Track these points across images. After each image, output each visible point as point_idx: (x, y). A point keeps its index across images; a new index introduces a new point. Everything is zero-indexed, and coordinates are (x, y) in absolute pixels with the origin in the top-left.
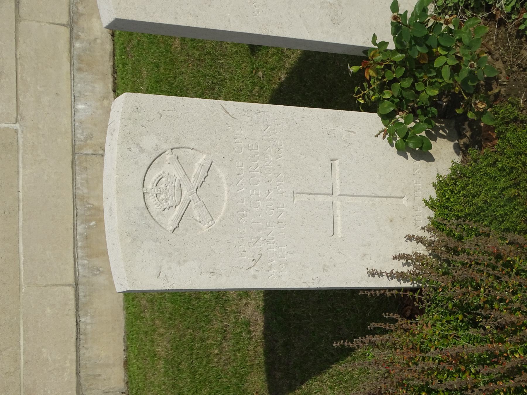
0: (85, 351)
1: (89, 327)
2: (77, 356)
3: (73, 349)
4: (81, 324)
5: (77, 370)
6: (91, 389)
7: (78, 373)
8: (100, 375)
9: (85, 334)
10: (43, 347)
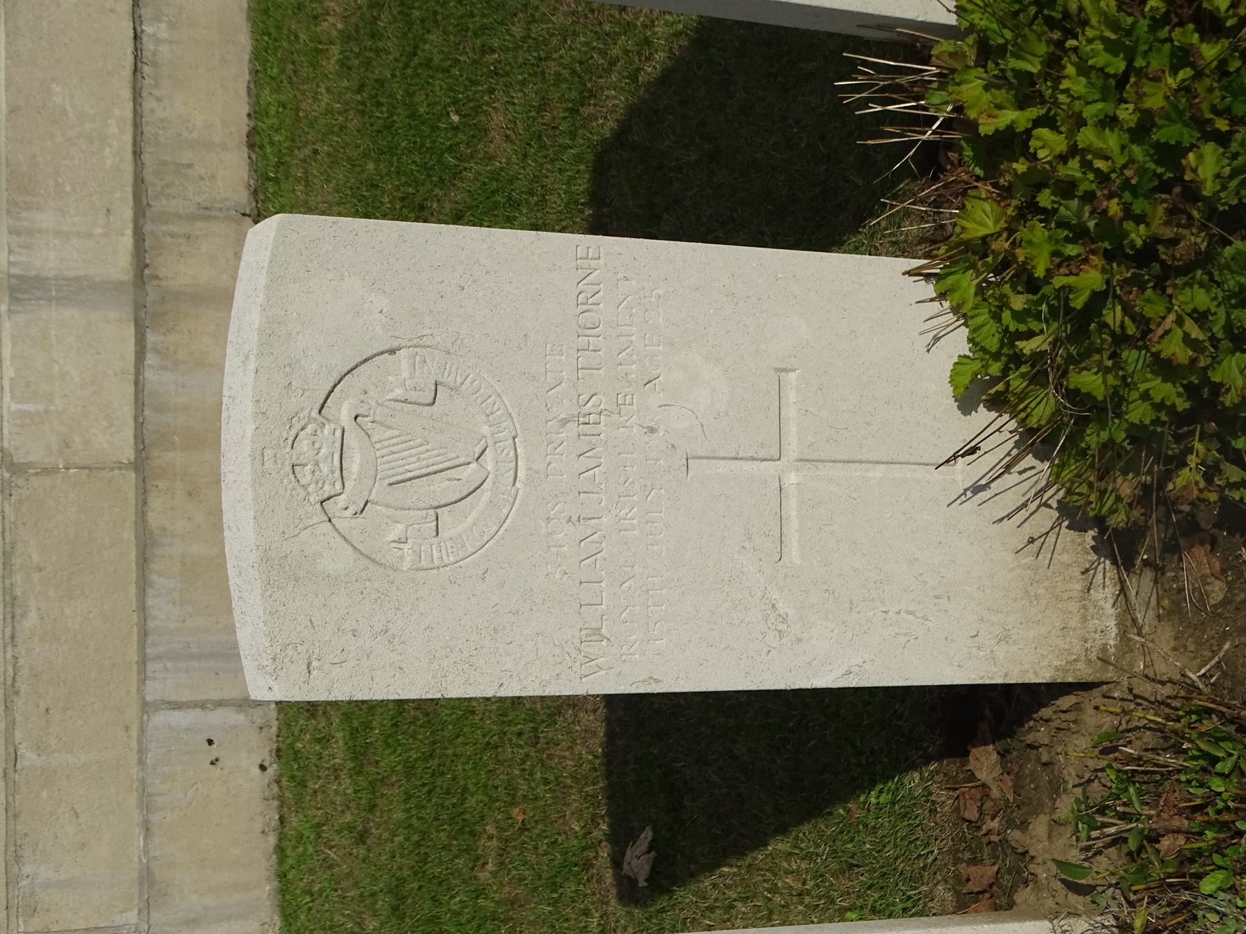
0: (154, 104)
1: (164, 49)
2: (135, 110)
3: (127, 93)
4: (145, 39)
5: (135, 144)
6: (168, 196)
7: (137, 153)
8: (190, 166)
9: (155, 64)
10: (53, 79)
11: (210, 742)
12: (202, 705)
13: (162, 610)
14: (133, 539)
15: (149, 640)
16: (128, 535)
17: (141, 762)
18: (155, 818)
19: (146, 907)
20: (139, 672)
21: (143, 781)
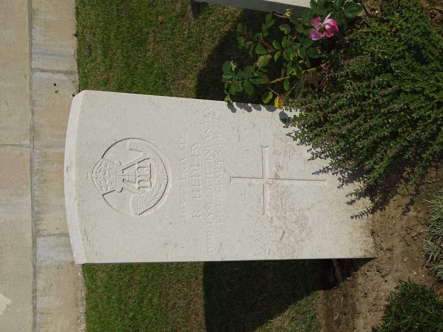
11: (55, 85)
12: (52, 72)
13: (38, 37)
14: (27, 11)
15: (33, 47)
16: (25, 9)
17: (30, 89)
18: (36, 109)
19: (32, 140)
20: (29, 58)
21: (31, 95)
